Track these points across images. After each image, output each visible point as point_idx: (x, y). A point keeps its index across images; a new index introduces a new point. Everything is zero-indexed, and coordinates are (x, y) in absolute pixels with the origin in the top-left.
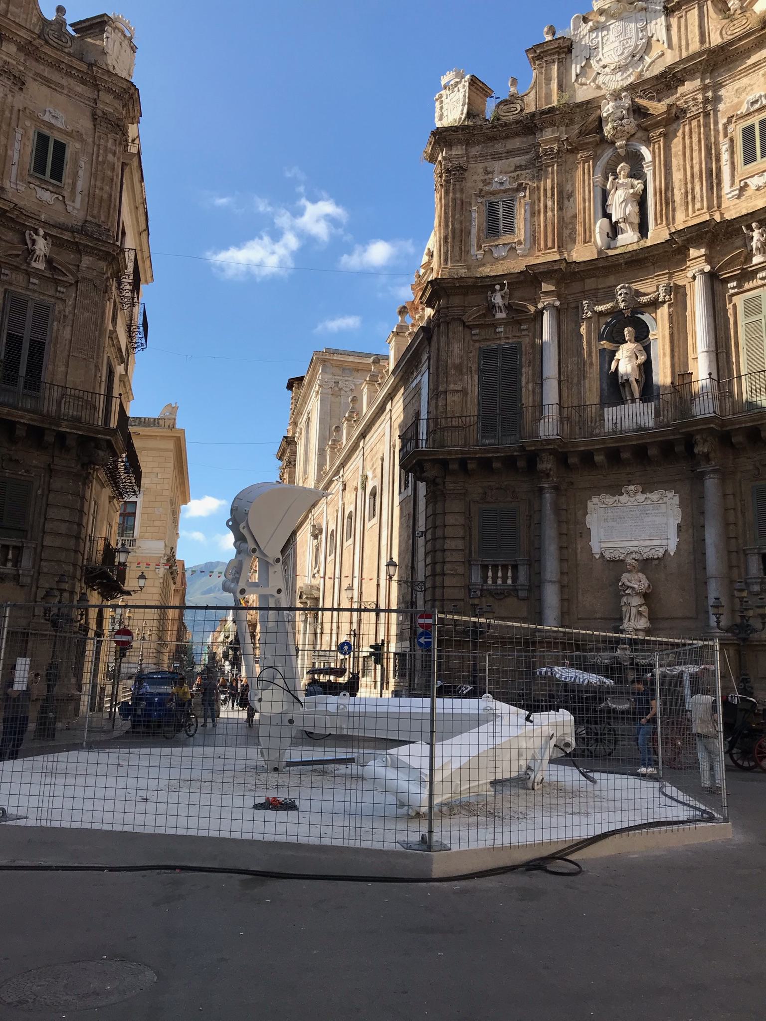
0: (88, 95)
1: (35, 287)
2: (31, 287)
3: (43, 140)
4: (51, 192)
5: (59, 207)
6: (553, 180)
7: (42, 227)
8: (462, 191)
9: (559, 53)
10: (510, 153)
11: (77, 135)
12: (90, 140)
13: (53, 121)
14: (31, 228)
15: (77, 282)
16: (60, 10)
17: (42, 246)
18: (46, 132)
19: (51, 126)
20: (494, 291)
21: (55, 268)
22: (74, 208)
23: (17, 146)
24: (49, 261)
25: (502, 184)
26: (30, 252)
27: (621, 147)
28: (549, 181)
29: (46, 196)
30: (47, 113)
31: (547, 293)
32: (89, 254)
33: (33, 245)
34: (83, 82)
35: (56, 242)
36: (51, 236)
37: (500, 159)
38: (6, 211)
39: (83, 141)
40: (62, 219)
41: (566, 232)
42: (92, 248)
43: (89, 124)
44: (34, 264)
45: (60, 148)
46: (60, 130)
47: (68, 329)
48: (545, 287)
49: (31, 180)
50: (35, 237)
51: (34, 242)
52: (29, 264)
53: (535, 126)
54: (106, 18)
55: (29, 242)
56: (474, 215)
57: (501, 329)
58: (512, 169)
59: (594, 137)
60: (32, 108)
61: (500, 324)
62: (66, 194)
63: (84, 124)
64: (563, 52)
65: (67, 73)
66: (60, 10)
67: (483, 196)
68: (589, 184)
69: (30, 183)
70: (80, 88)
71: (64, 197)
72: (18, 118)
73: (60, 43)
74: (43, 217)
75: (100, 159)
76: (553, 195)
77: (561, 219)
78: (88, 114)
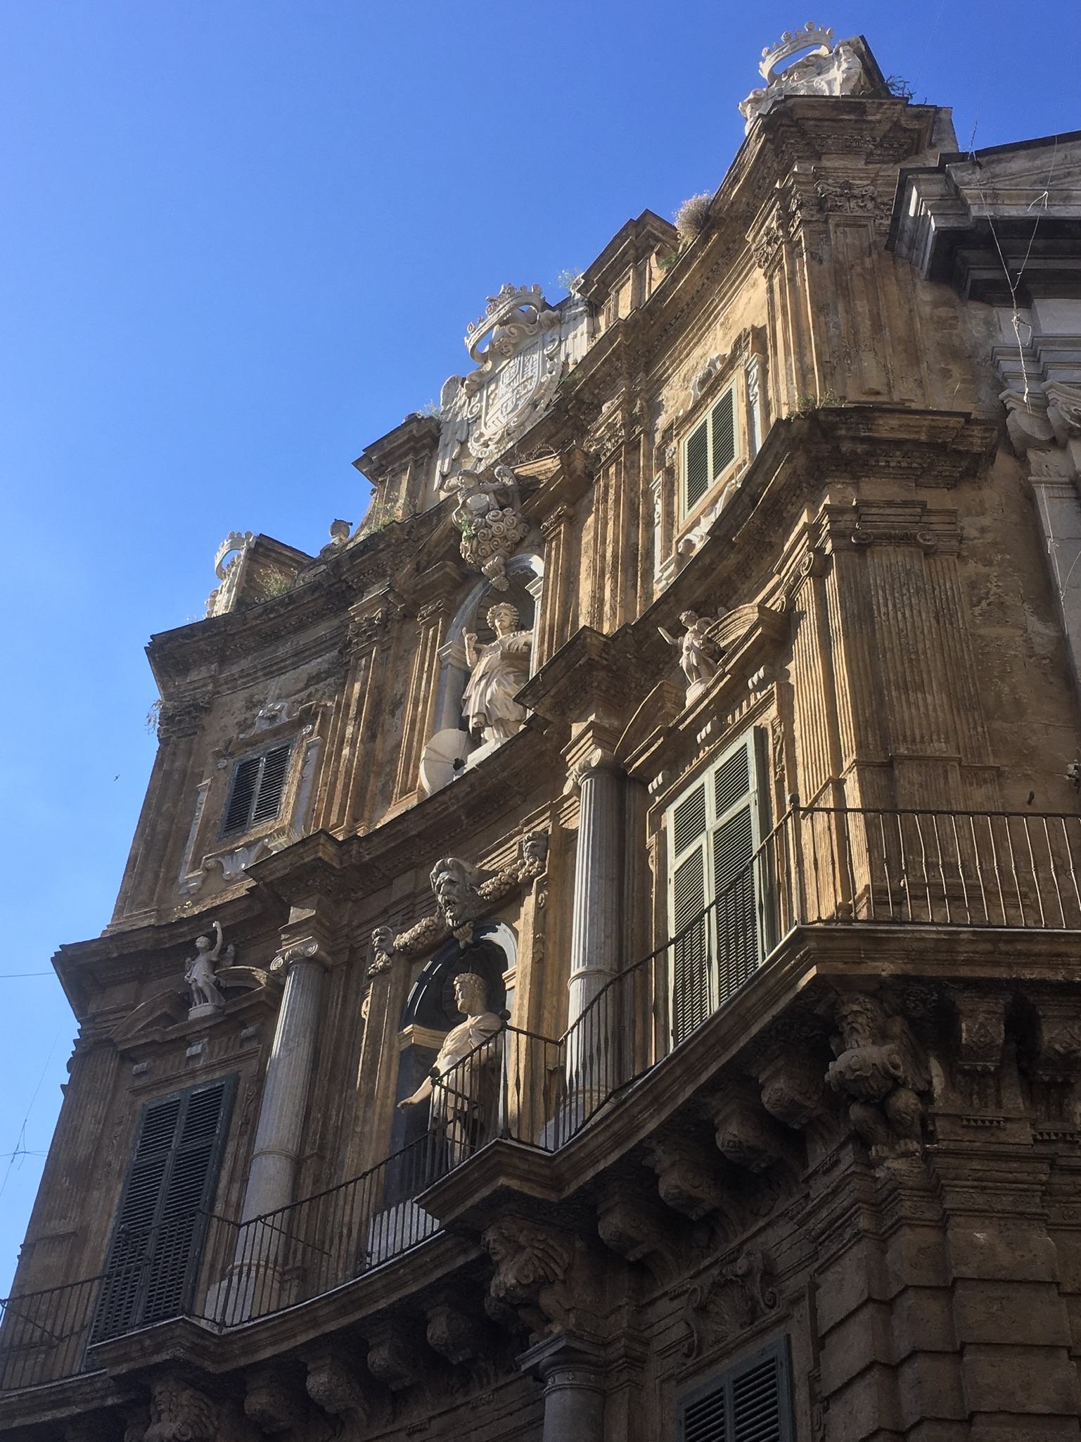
6: (364, 684)
8: (189, 753)
9: (416, 451)
10: (300, 656)
20: (195, 953)
25: (273, 718)
27: (495, 572)
28: (357, 686)
31: (297, 929)
37: (281, 671)
41: (374, 785)
48: (296, 915)
53: (350, 587)
56: (203, 797)
57: (195, 1049)
58: (302, 685)
59: (441, 567)
61: (198, 1036)
64: (424, 447)
67: (232, 755)
68: (430, 665)
76: (359, 712)
77: (368, 759)
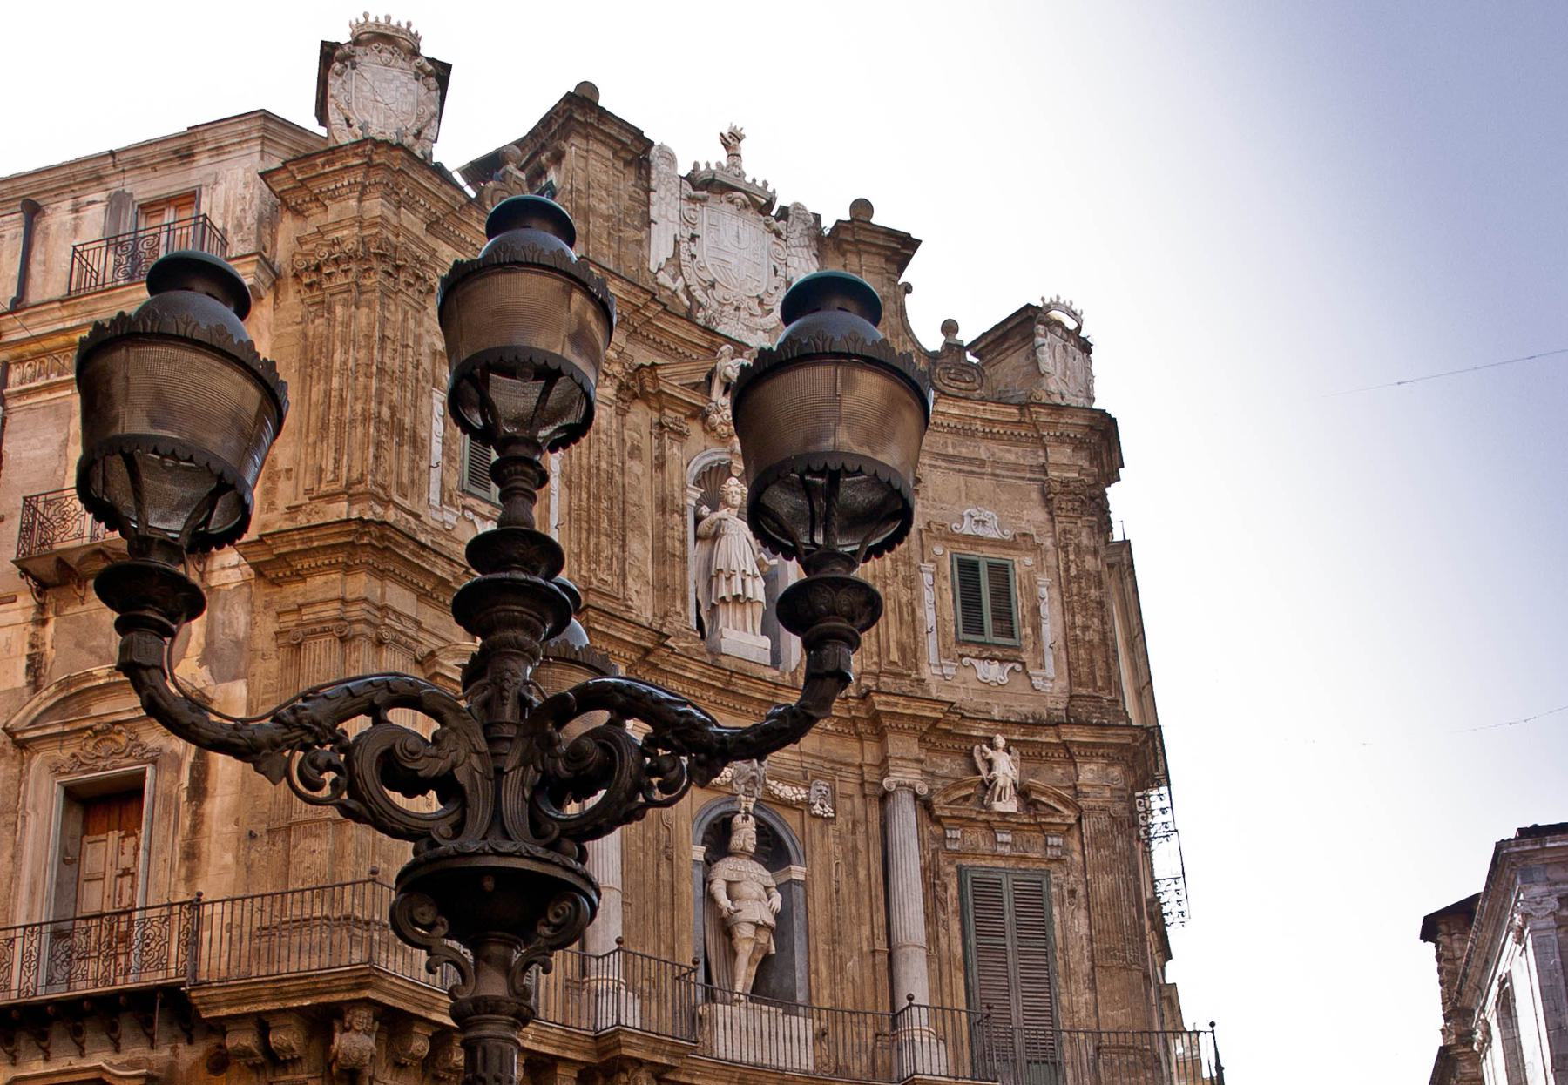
0: (1029, 461)
1: (1007, 850)
2: (1000, 849)
3: (967, 569)
4: (1001, 661)
5: (1021, 684)
7: (1001, 732)
11: (1022, 542)
12: (1048, 543)
13: (980, 531)
14: (979, 740)
15: (1079, 820)
16: (949, 327)
17: (1006, 769)
18: (970, 553)
19: (976, 540)
21: (1035, 803)
22: (1045, 678)
23: (928, 596)
24: (1023, 793)
26: (988, 785)
29: (993, 672)
30: (967, 519)
32: (1088, 759)
33: (990, 770)
34: (1014, 440)
35: (1029, 753)
36: (1017, 743)
38: (938, 720)
39: (1036, 548)
40: (1026, 707)
42: (1094, 745)
43: (1040, 515)
44: (998, 806)
45: (1001, 572)
46: (993, 543)
47: (1082, 914)
49: (964, 650)
50: (991, 754)
51: (990, 764)
52: (989, 808)
54: (1030, 313)
55: (982, 766)
60: (939, 520)
62: (1025, 657)
63: (1034, 516)
65: (985, 435)
66: (949, 327)
69: (962, 656)
70: (1011, 455)
71: (1023, 664)
72: (922, 546)
73: (963, 385)
74: (996, 714)
75: (1073, 572)
78: (1035, 496)
